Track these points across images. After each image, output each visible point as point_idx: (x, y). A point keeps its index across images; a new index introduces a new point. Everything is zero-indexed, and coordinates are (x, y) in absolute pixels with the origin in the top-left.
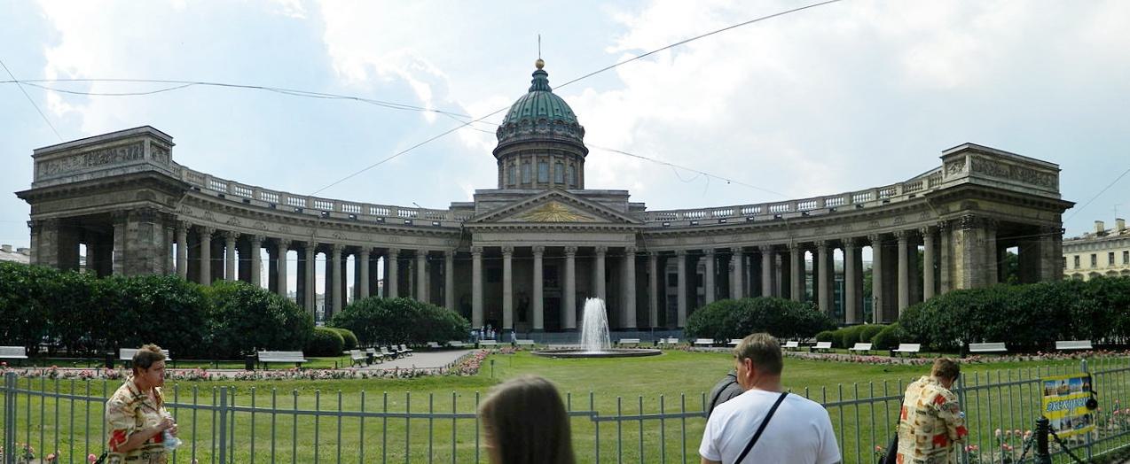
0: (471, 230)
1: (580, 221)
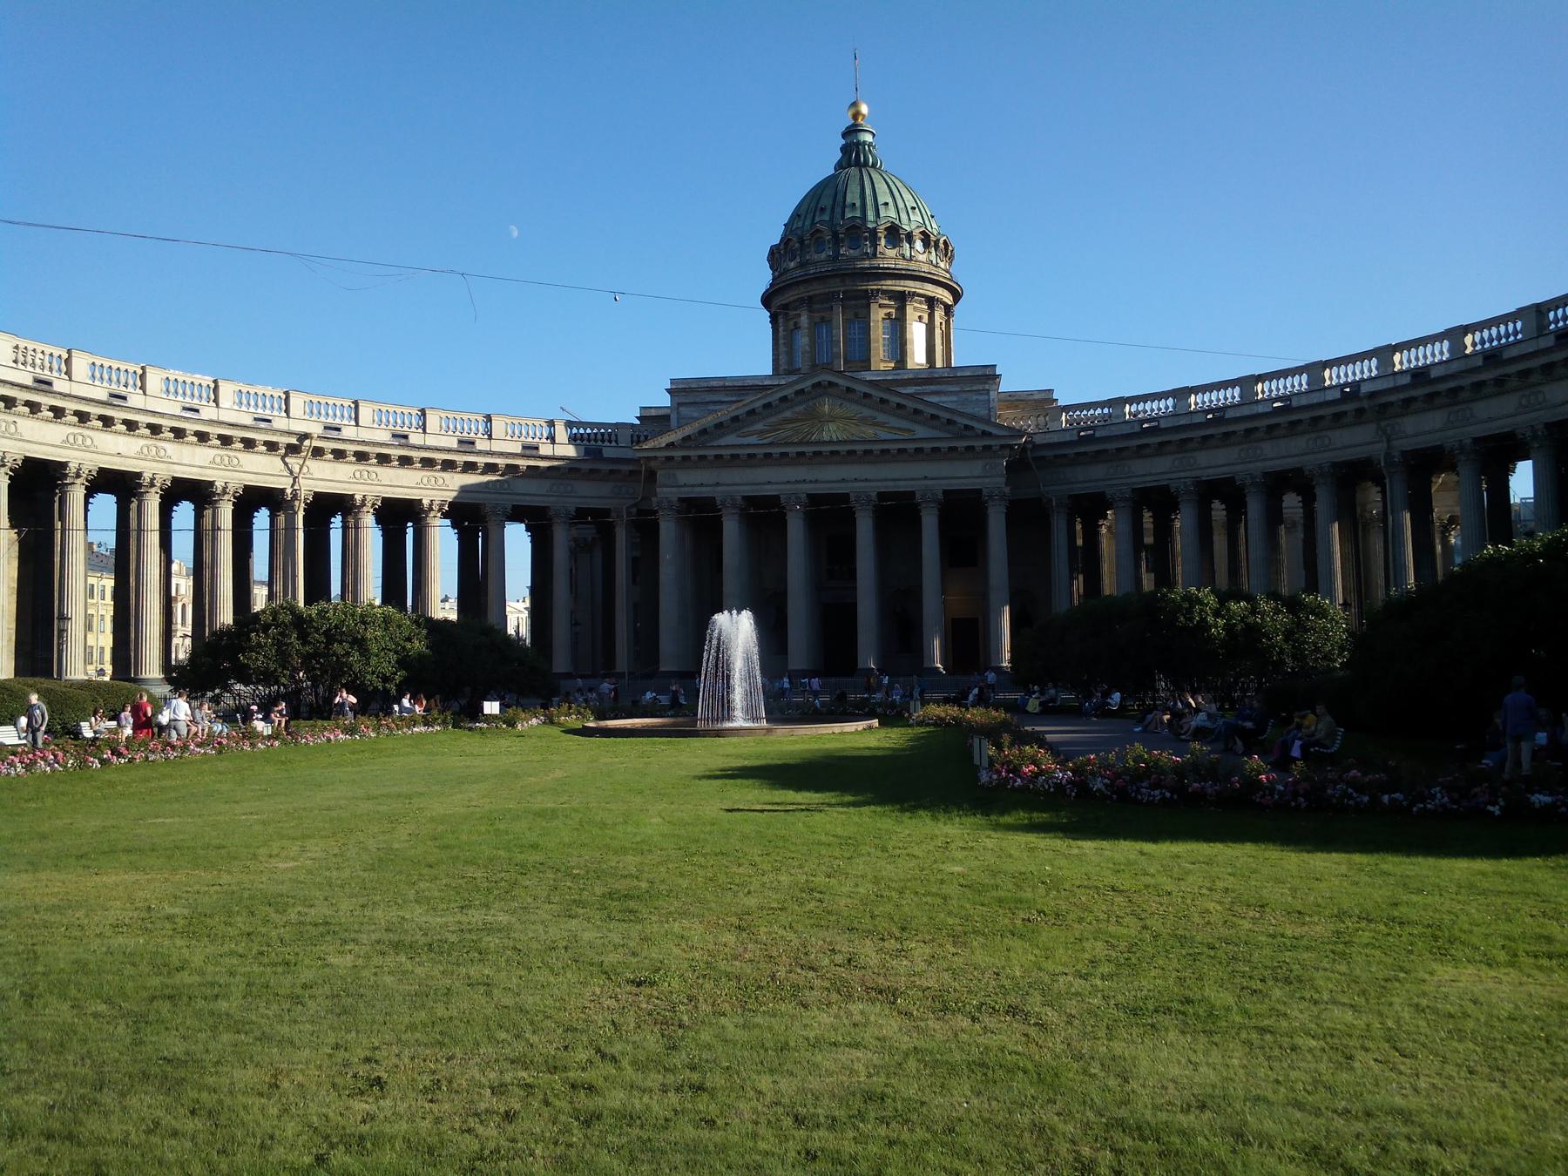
0: (653, 464)
1: (883, 435)
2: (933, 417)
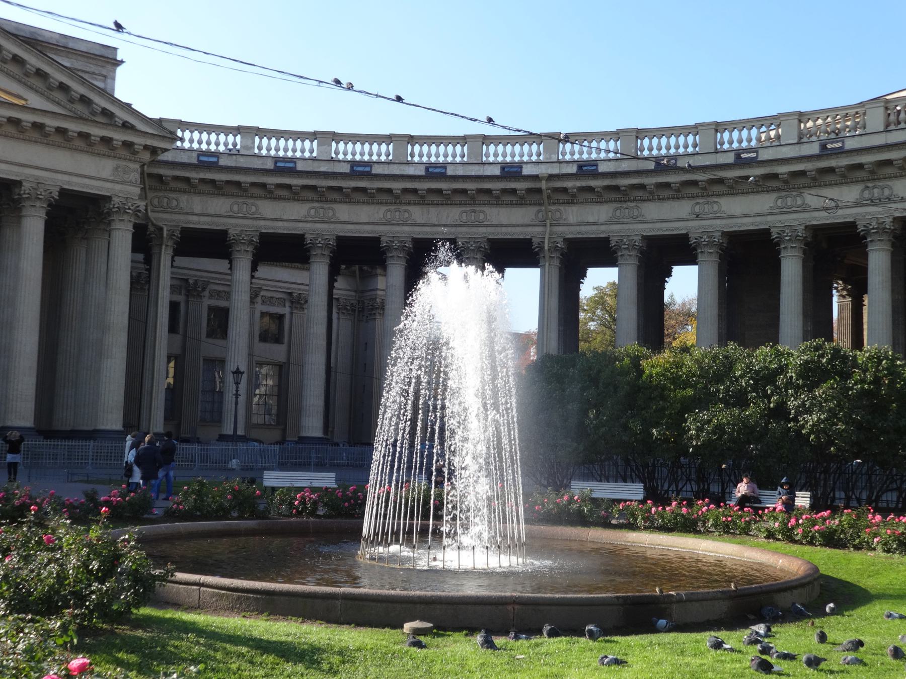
2: (63, 87)
